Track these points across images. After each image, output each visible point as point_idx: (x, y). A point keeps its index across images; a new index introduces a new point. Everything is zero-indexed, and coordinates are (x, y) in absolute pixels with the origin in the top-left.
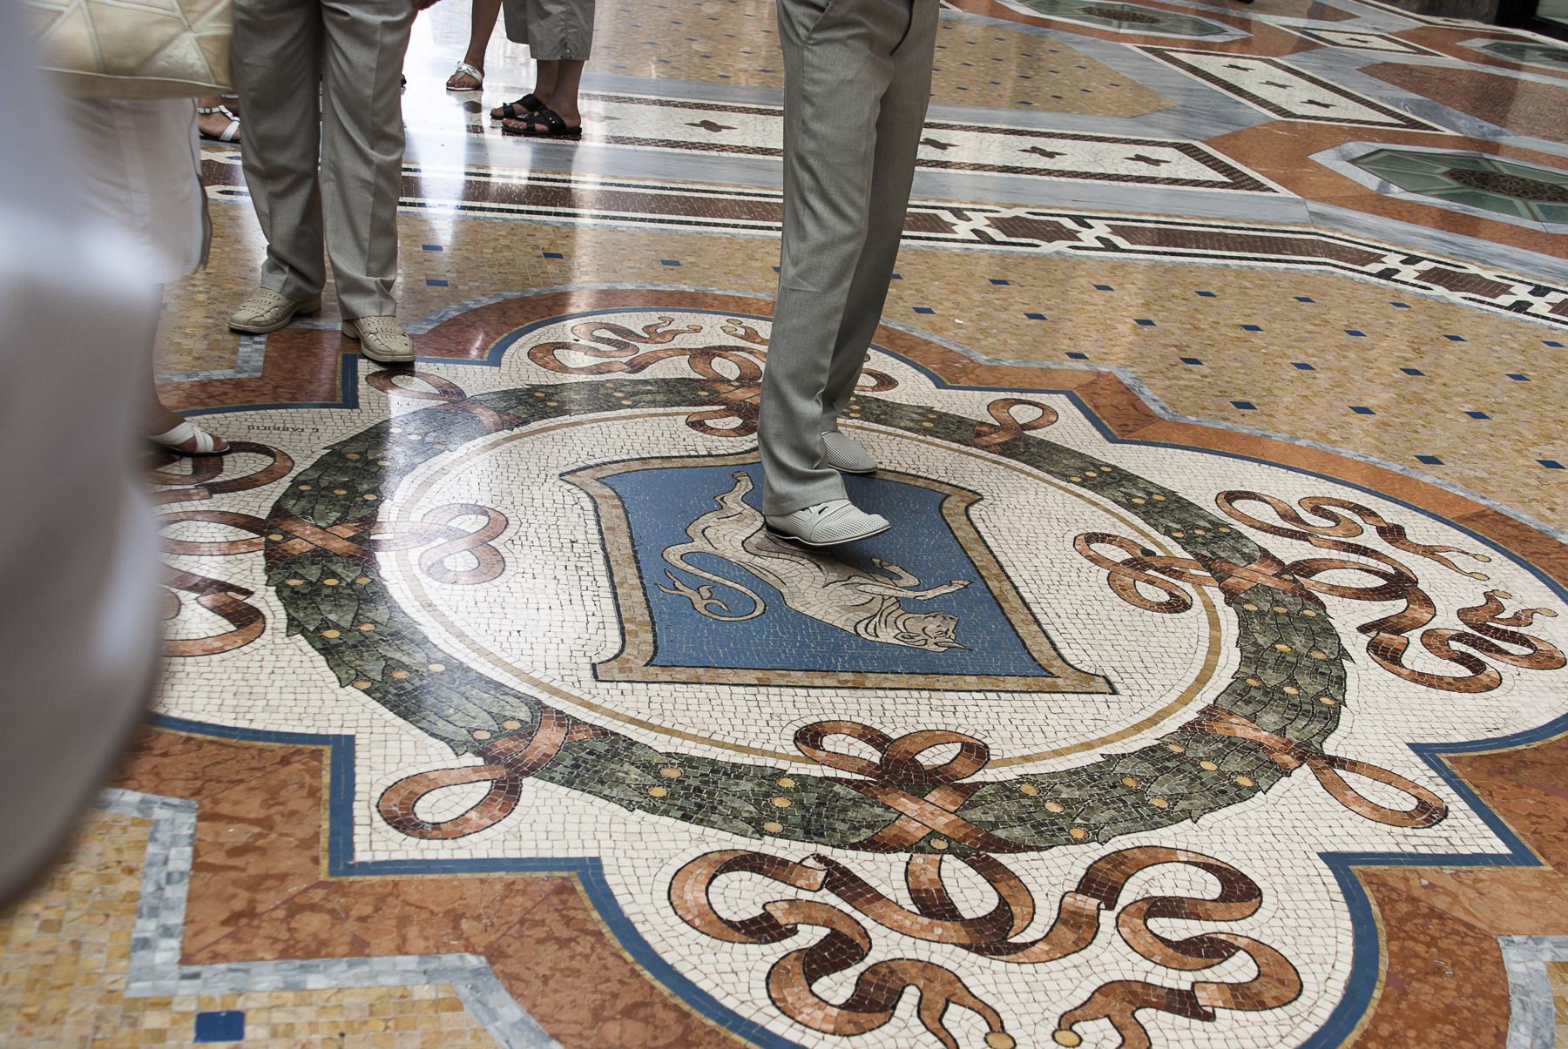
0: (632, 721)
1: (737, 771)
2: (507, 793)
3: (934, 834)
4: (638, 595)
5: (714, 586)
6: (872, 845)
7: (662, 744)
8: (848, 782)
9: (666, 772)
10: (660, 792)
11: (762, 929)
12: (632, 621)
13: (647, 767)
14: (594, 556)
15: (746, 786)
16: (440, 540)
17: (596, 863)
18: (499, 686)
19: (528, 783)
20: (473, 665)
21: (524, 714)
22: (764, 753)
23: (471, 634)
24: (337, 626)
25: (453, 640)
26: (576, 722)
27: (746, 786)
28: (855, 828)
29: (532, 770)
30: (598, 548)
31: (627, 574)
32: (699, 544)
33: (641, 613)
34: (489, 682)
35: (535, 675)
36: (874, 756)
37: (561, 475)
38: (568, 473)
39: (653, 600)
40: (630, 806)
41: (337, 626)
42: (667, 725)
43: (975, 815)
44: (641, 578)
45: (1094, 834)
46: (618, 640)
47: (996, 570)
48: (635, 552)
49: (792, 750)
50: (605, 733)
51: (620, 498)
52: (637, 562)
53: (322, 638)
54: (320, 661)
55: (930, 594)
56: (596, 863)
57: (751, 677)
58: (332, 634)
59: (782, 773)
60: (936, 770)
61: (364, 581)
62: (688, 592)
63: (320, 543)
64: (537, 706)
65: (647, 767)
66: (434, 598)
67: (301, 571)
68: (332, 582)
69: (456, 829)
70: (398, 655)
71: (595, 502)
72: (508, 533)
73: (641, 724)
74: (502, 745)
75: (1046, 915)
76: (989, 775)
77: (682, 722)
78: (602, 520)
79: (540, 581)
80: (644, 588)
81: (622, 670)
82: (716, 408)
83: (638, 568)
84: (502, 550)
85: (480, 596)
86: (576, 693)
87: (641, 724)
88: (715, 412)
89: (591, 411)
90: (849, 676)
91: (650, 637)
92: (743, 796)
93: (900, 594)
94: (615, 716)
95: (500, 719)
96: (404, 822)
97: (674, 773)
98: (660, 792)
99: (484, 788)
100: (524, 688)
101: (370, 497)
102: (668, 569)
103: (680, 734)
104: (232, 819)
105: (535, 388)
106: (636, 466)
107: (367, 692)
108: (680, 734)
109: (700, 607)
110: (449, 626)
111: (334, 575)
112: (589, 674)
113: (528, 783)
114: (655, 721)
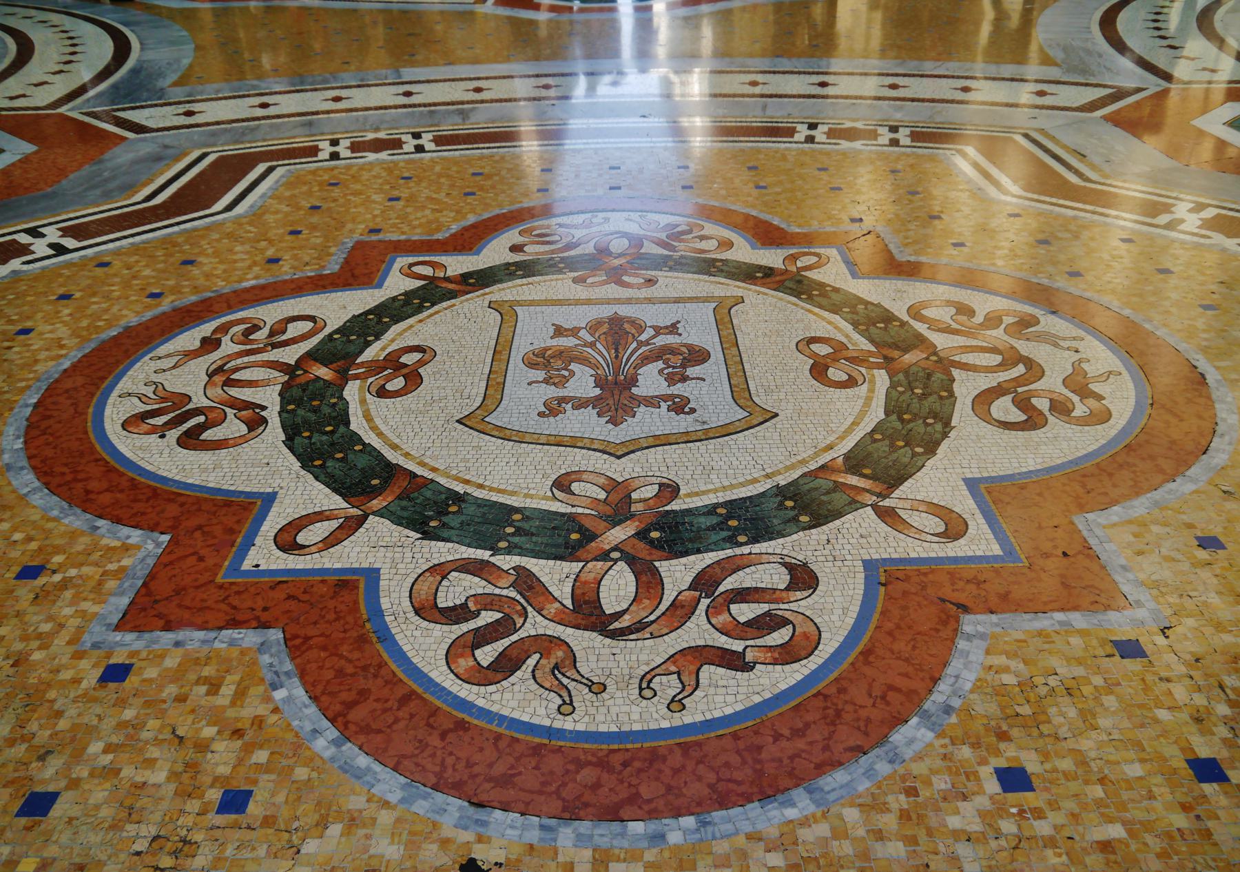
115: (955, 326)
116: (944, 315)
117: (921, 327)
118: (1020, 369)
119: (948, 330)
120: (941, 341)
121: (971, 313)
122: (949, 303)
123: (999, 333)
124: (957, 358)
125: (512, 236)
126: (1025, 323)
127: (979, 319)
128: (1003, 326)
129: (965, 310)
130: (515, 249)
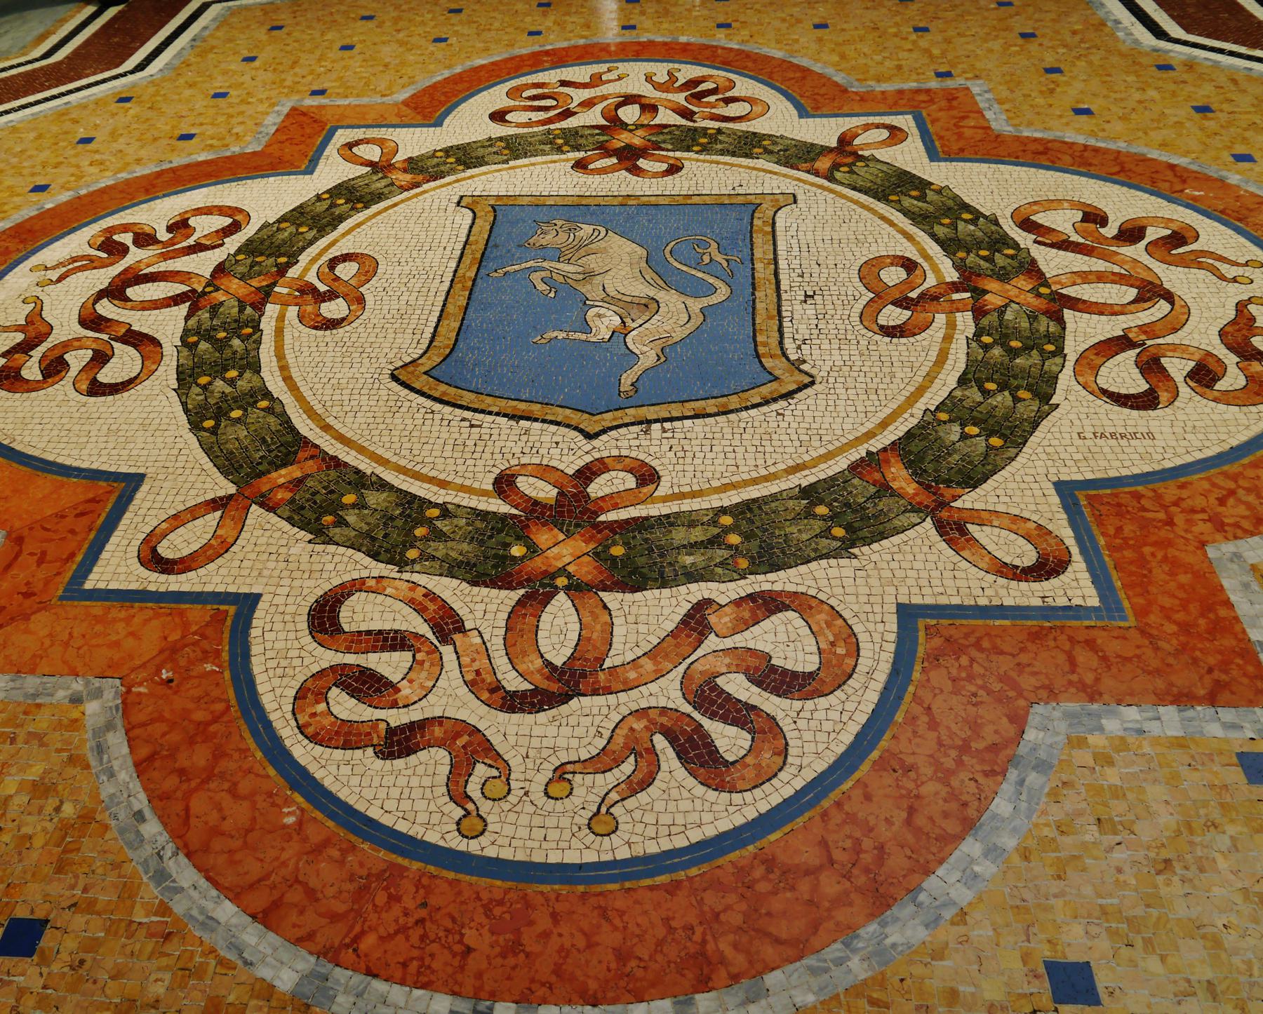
0: (775, 173)
1: (722, 152)
2: (845, 141)
3: (631, 131)
4: (758, 254)
5: (698, 265)
6: (665, 126)
7: (761, 163)
8: (663, 150)
9: (761, 150)
10: (765, 143)
11: (728, 101)
12: (766, 233)
13: (771, 152)
14: (788, 288)
15: (719, 146)
16: (914, 295)
17: (801, 116)
18: (854, 189)
19: (834, 144)
20: (871, 200)
21: (838, 175)
22: (704, 161)
23: (876, 219)
24: (966, 221)
25: (887, 215)
26: (808, 172)
27: (719, 146)
28: (670, 133)
29: (831, 150)
30: (784, 296)
31: (764, 272)
32: (696, 305)
33: (758, 239)
34: (860, 191)
35: (832, 196)
36: (642, 163)
37: (813, 383)
38: (806, 386)
39: (747, 251)
40: (782, 137)
41: (966, 221)
42: (755, 172)
43: (602, 138)
44: (753, 269)
45: (549, 132)
46: (777, 219)
47: (458, 286)
48: (753, 294)
49: (686, 163)
50: (792, 167)
51: (758, 356)
52: (753, 284)
53: (971, 213)
54: (967, 200)
55: (531, 264)
56: (801, 116)
57: (696, 200)
58: (967, 216)
59: (697, 152)
60: (610, 156)
61: (961, 254)
62: (719, 258)
63: (1008, 287)
64: (830, 178)
65: (771, 152)
66: (908, 244)
67: (1009, 261)
68: (984, 253)
69: (867, 127)
70: (920, 204)
71: (782, 349)
72: (859, 306)
73: (771, 172)
74: (849, 160)
75: (599, 108)
76: (581, 155)
77: (744, 174)
78: (776, 328)
79: (831, 262)
80: (752, 260)
81: (777, 200)
82: (612, 516)
83: (753, 278)
84: (862, 289)
85: (874, 247)
86: (807, 187)
87: (771, 172)
88: (616, 507)
89: (774, 497)
90: (630, 202)
91: (756, 222)
92: (721, 142)
93: (554, 264)
94: (785, 176)
95: (851, 172)
96: (892, 129)
97: (756, 150)
98: (765, 143)
99: (856, 142)
100: (839, 188)
101: (987, 339)
102: (729, 277)
103: (749, 168)
104: (974, 127)
105: (845, 548)
106: (734, 402)
107: (932, 184)
108: (749, 168)
109: (714, 245)
110: (891, 224)
111: (983, 258)
112: (799, 197)
113: (834, 144)
114: (762, 174)
115: (1075, 238)
116: (1064, 222)
117: (1024, 239)
118: (1163, 307)
119: (1065, 245)
120: (1052, 262)
121: (1103, 221)
122: (1075, 205)
123: (1136, 251)
124: (1071, 291)
125: (496, 97)
126: (1178, 238)
127: (1110, 231)
128: (1144, 243)
129: (1094, 217)
130: (498, 117)
